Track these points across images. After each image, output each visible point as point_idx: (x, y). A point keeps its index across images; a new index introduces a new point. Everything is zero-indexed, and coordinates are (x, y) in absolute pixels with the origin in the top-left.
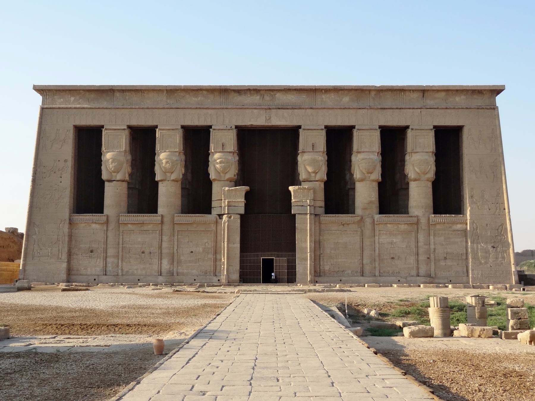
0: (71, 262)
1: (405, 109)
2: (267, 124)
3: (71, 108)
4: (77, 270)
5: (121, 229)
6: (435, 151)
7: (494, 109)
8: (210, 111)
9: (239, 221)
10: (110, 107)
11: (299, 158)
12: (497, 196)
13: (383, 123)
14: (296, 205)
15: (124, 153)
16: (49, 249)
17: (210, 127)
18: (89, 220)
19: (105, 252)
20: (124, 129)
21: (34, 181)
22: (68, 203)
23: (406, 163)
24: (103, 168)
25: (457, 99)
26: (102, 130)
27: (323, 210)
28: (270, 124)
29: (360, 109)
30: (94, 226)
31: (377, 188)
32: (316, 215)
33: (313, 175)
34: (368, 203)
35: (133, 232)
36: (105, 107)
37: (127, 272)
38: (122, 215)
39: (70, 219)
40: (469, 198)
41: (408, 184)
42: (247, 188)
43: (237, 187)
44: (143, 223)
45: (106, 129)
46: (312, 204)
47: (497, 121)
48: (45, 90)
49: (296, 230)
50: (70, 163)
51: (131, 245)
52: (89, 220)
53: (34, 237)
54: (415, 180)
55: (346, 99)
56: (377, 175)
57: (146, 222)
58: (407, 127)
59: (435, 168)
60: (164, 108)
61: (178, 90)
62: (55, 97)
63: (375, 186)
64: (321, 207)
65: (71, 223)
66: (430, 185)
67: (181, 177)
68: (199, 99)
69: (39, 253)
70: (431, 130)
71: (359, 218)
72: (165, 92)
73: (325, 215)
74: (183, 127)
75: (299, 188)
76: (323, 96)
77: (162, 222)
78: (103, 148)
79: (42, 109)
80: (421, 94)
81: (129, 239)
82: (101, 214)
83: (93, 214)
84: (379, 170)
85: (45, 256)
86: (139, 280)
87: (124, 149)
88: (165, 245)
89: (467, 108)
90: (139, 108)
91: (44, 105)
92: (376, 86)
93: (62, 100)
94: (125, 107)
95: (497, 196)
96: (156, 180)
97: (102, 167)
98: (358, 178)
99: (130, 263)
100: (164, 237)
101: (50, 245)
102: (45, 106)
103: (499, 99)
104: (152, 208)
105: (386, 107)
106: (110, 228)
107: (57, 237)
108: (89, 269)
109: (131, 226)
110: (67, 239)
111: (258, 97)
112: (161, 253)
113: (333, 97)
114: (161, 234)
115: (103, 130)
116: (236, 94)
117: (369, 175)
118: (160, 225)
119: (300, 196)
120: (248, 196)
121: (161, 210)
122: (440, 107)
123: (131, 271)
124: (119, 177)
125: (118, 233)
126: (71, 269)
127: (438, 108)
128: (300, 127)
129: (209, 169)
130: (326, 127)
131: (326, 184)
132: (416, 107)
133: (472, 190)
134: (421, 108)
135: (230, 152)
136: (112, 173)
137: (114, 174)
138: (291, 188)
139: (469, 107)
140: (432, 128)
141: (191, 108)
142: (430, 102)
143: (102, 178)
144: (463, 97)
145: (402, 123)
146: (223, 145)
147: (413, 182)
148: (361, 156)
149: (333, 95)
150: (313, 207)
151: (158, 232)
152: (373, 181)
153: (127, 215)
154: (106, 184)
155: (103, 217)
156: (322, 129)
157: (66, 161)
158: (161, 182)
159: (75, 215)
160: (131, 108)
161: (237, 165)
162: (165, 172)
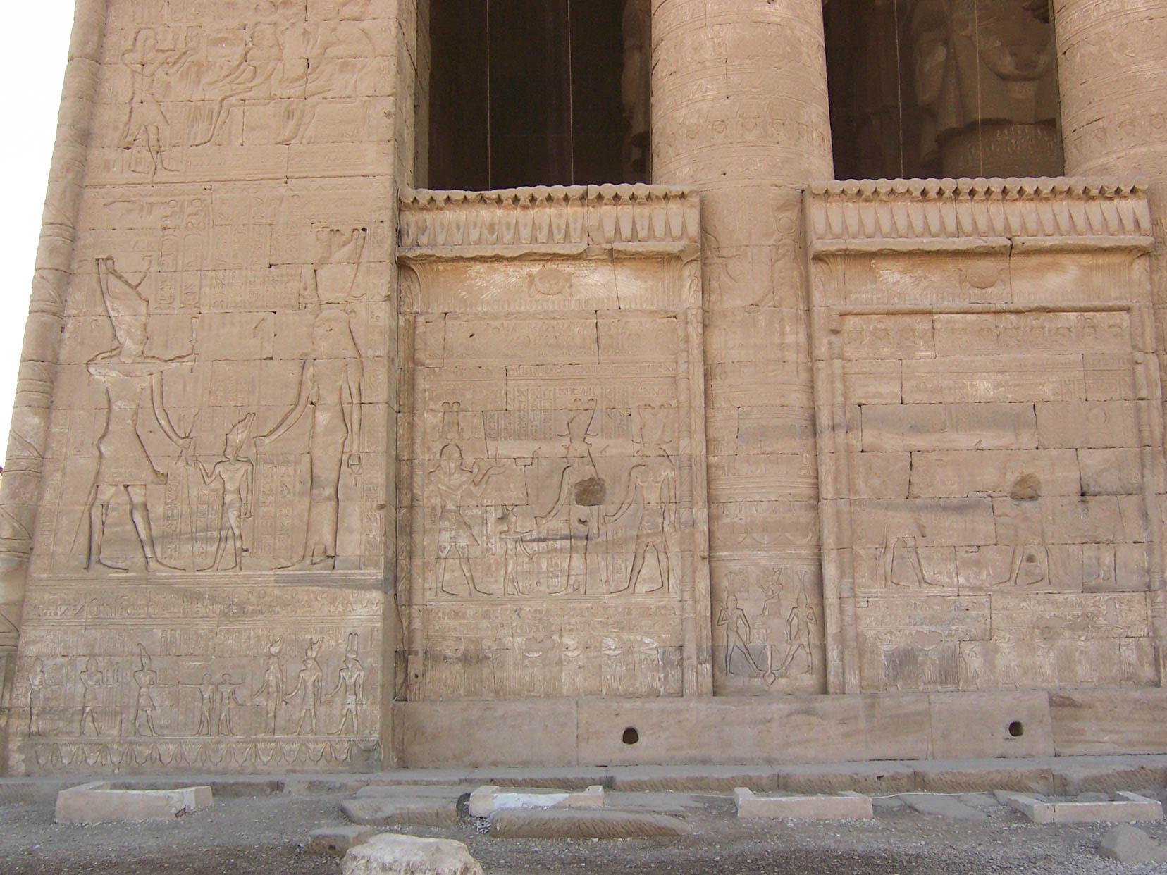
0: (418, 583)
4: (472, 659)
16: (234, 476)
18: (559, 236)
19: (701, 493)
22: (388, 104)
35: (921, 324)
37: (904, 661)
39: (399, 233)
44: (1009, 251)
51: (916, 429)
52: (559, 236)
53: (104, 375)
69: (145, 506)
81: (889, 389)
85: (193, 540)
86: (1015, 729)
99: (923, 581)
101: (239, 436)
106: (732, 301)
107: (292, 371)
108: (567, 640)
109: (907, 279)
110: (379, 388)
123: (932, 652)
125: (802, 338)
126: (418, 645)
155: (674, 207)
159: (441, 195)
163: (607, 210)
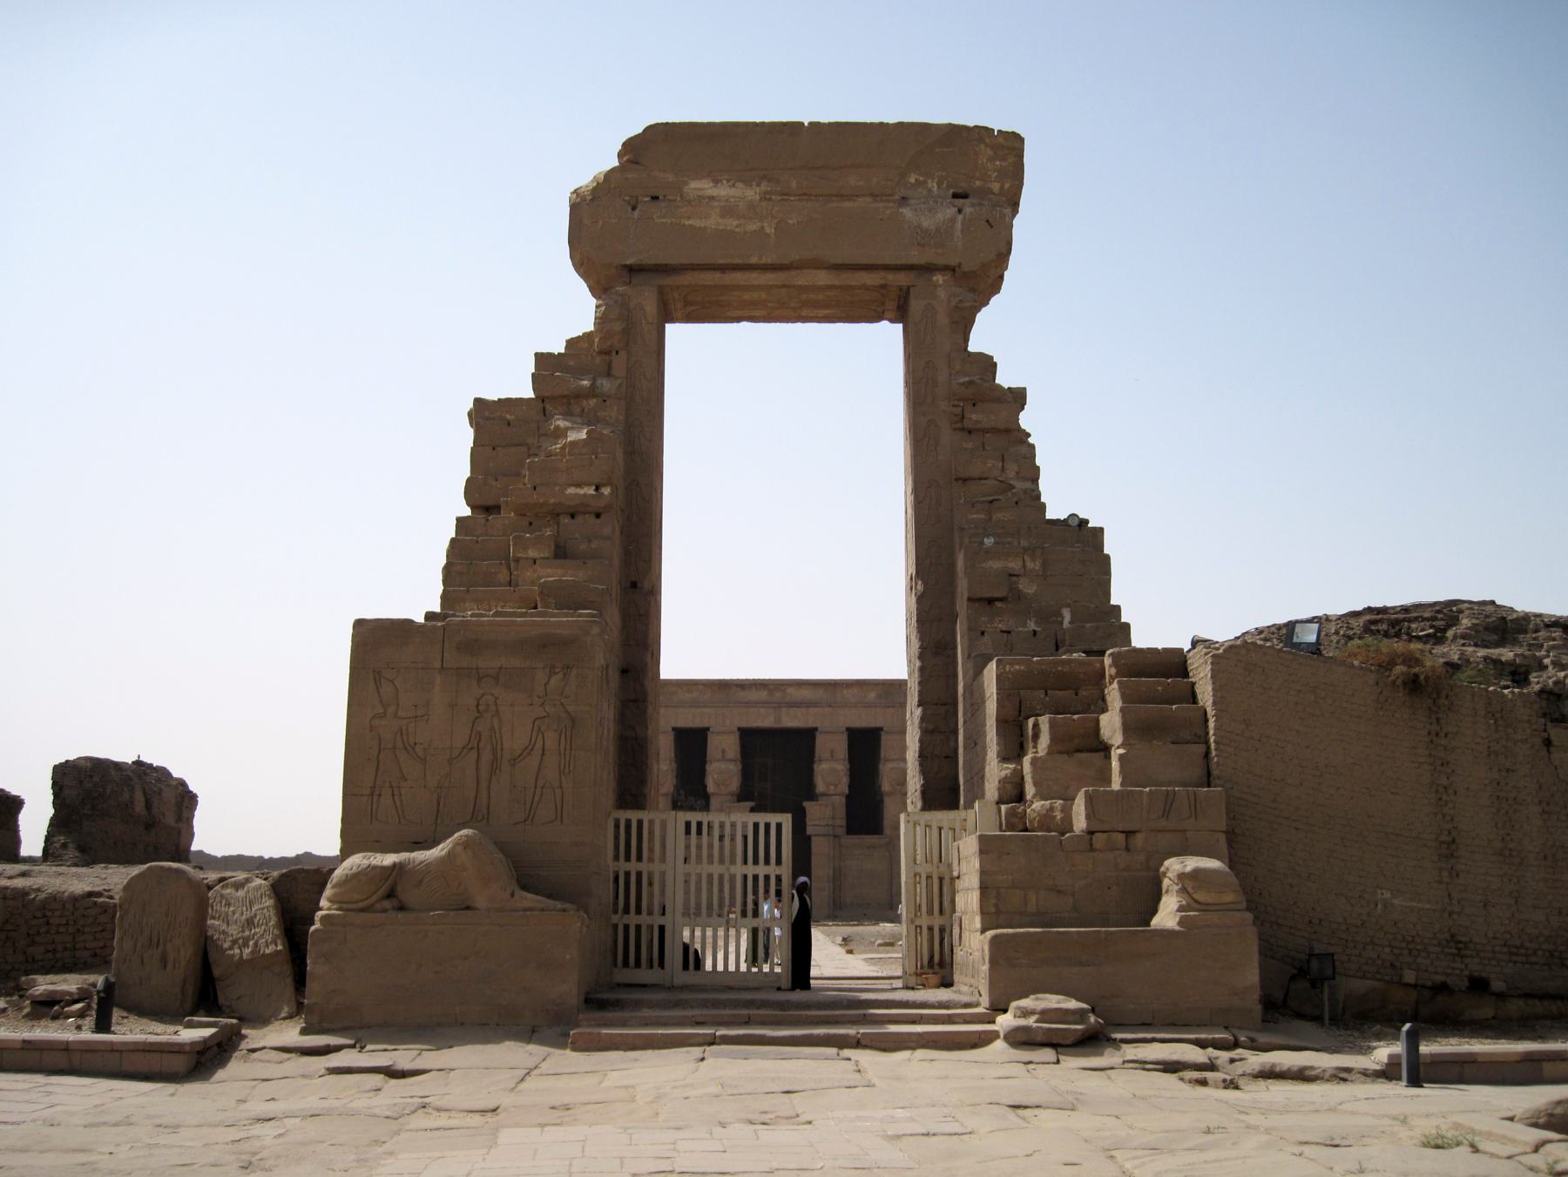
2: (776, 726)
8: (706, 710)
11: (815, 766)
17: (708, 729)
27: (844, 830)
28: (779, 726)
29: (889, 707)
32: (835, 836)
33: (832, 787)
43: (740, 804)
46: (831, 822)
49: (813, 857)
64: (841, 826)
67: (672, 788)
71: (887, 840)
73: (849, 836)
74: (674, 729)
76: (845, 692)
111: (766, 693)
113: (856, 691)
116: (739, 689)
128: (816, 729)
129: (706, 780)
130: (849, 730)
131: (848, 798)
135: (731, 760)
138: (806, 804)
146: (723, 751)
148: (890, 765)
149: (856, 690)
150: (831, 828)
156: (843, 732)
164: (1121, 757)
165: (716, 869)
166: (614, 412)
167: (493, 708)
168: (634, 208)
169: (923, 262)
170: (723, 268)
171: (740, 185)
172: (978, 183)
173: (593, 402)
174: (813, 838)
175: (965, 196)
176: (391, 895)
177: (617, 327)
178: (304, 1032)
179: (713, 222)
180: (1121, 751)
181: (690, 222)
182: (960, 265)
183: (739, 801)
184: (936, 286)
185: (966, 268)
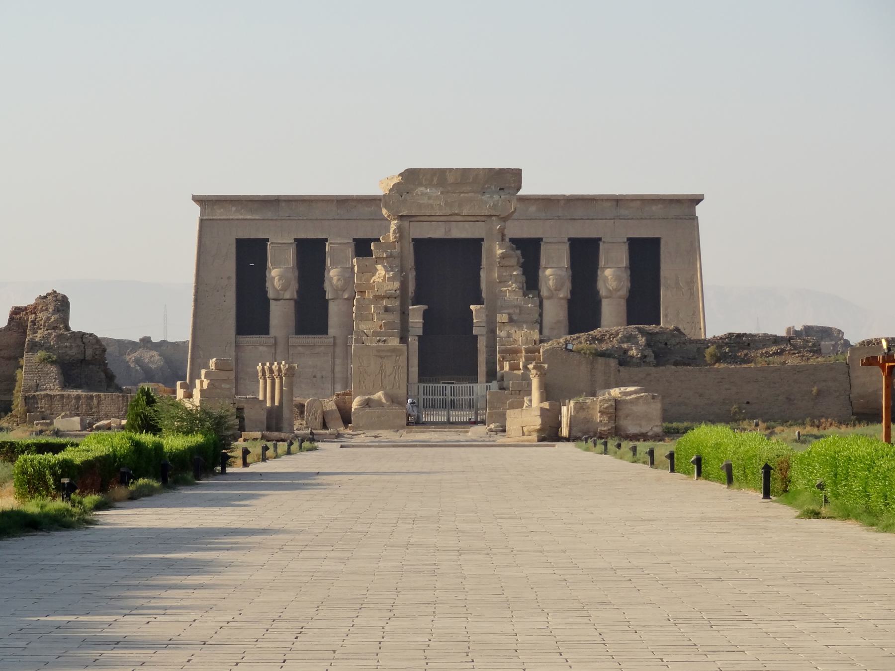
1: (597, 219)
2: (445, 237)
3: (232, 219)
5: (291, 352)
6: (628, 265)
7: (694, 219)
9: (417, 343)
10: (275, 218)
12: (694, 314)
13: (574, 235)
14: (478, 325)
15: (291, 270)
20: (291, 243)
21: (196, 300)
23: (598, 278)
24: (268, 284)
25: (654, 208)
26: (267, 244)
30: (261, 348)
31: (567, 306)
34: (555, 323)
36: (270, 218)
38: (292, 336)
40: (663, 317)
41: (600, 301)
42: (426, 307)
43: (415, 307)
44: (315, 345)
45: (272, 243)
47: (696, 233)
48: (204, 201)
50: (233, 281)
54: (607, 297)
55: (533, 209)
56: (565, 293)
57: (317, 344)
58: (600, 239)
59: (629, 285)
60: (334, 219)
61: (350, 200)
62: (215, 207)
63: (565, 304)
65: (237, 346)
66: (623, 303)
68: (372, 208)
70: (625, 243)
72: (336, 201)
75: (481, 308)
77: (335, 344)
78: (269, 264)
79: (202, 221)
80: (615, 203)
82: (267, 336)
83: (261, 336)
84: (568, 285)
87: (292, 265)
88: (338, 369)
89: (664, 219)
90: (307, 220)
91: (203, 216)
92: (564, 195)
93: (222, 210)
94: (292, 218)
95: (694, 314)
96: (327, 298)
97: (267, 284)
98: (544, 295)
100: (336, 360)
102: (205, 218)
103: (699, 209)
104: (322, 328)
105: (576, 218)
112: (334, 377)
114: (333, 357)
115: (269, 244)
117: (557, 292)
118: (333, 347)
119: (482, 316)
120: (426, 314)
121: (332, 331)
122: (634, 217)
124: (287, 295)
127: (632, 219)
132: (608, 218)
133: (666, 309)
134: (614, 219)
136: (280, 292)
137: (282, 292)
138: (472, 307)
139: (666, 217)
140: (626, 241)
141: (364, 219)
142: (624, 212)
143: (268, 295)
144: (660, 206)
145: (594, 235)
147: (604, 299)
151: (330, 354)
152: (561, 298)
153: (294, 336)
154: (272, 303)
157: (229, 278)
158: (332, 301)
160: (299, 220)
161: (414, 277)
162: (336, 290)
163: (263, 339)
164: (522, 373)
165: (431, 397)
166: (397, 262)
167: (384, 365)
168: (401, 197)
169: (489, 214)
170: (429, 216)
171: (434, 189)
172: (507, 185)
173: (391, 259)
174: (478, 336)
175: (503, 189)
176: (367, 404)
177: (398, 235)
178: (352, 431)
179: (425, 201)
180: (522, 371)
181: (419, 201)
182: (500, 215)
183: (413, 306)
184: (493, 220)
185: (502, 216)
